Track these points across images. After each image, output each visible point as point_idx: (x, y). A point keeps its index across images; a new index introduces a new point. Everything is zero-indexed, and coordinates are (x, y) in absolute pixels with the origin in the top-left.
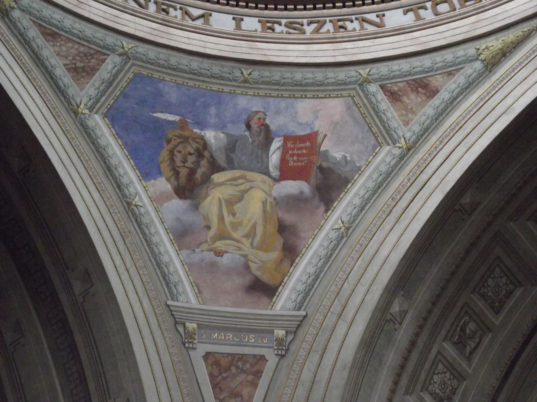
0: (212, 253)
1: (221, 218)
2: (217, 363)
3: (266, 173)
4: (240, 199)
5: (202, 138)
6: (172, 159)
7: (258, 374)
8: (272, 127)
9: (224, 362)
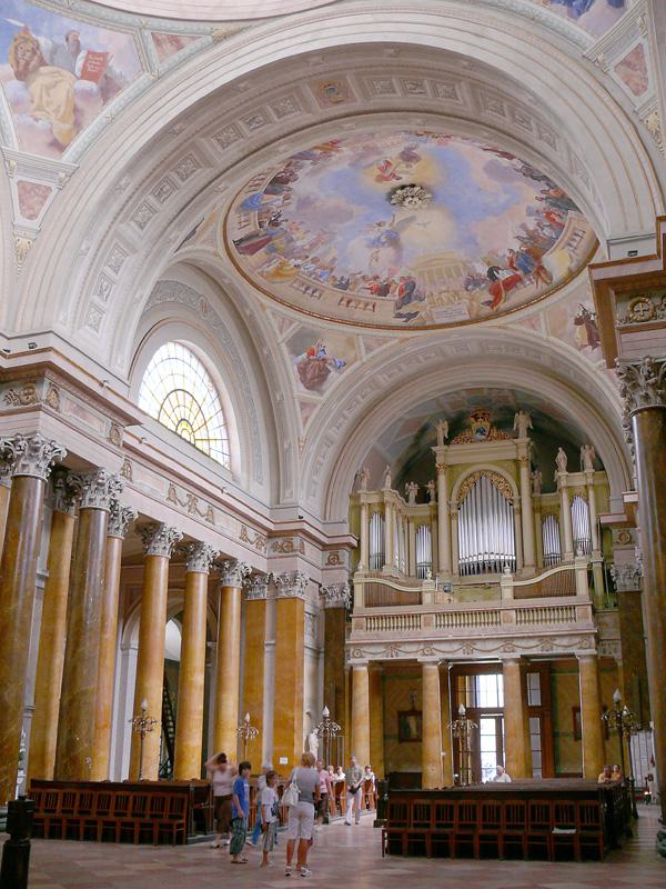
0: (32, 119)
1: (41, 97)
2: (23, 188)
3: (73, 73)
4: (54, 86)
5: (37, 41)
6: (16, 53)
7: (45, 198)
8: (82, 43)
9: (29, 188)
